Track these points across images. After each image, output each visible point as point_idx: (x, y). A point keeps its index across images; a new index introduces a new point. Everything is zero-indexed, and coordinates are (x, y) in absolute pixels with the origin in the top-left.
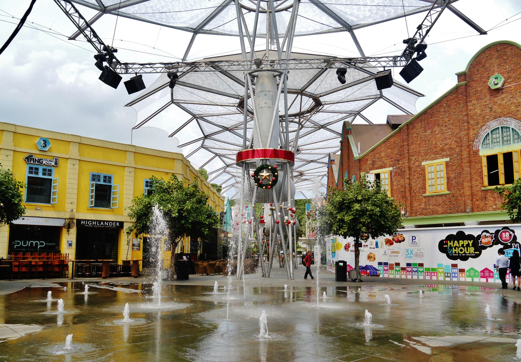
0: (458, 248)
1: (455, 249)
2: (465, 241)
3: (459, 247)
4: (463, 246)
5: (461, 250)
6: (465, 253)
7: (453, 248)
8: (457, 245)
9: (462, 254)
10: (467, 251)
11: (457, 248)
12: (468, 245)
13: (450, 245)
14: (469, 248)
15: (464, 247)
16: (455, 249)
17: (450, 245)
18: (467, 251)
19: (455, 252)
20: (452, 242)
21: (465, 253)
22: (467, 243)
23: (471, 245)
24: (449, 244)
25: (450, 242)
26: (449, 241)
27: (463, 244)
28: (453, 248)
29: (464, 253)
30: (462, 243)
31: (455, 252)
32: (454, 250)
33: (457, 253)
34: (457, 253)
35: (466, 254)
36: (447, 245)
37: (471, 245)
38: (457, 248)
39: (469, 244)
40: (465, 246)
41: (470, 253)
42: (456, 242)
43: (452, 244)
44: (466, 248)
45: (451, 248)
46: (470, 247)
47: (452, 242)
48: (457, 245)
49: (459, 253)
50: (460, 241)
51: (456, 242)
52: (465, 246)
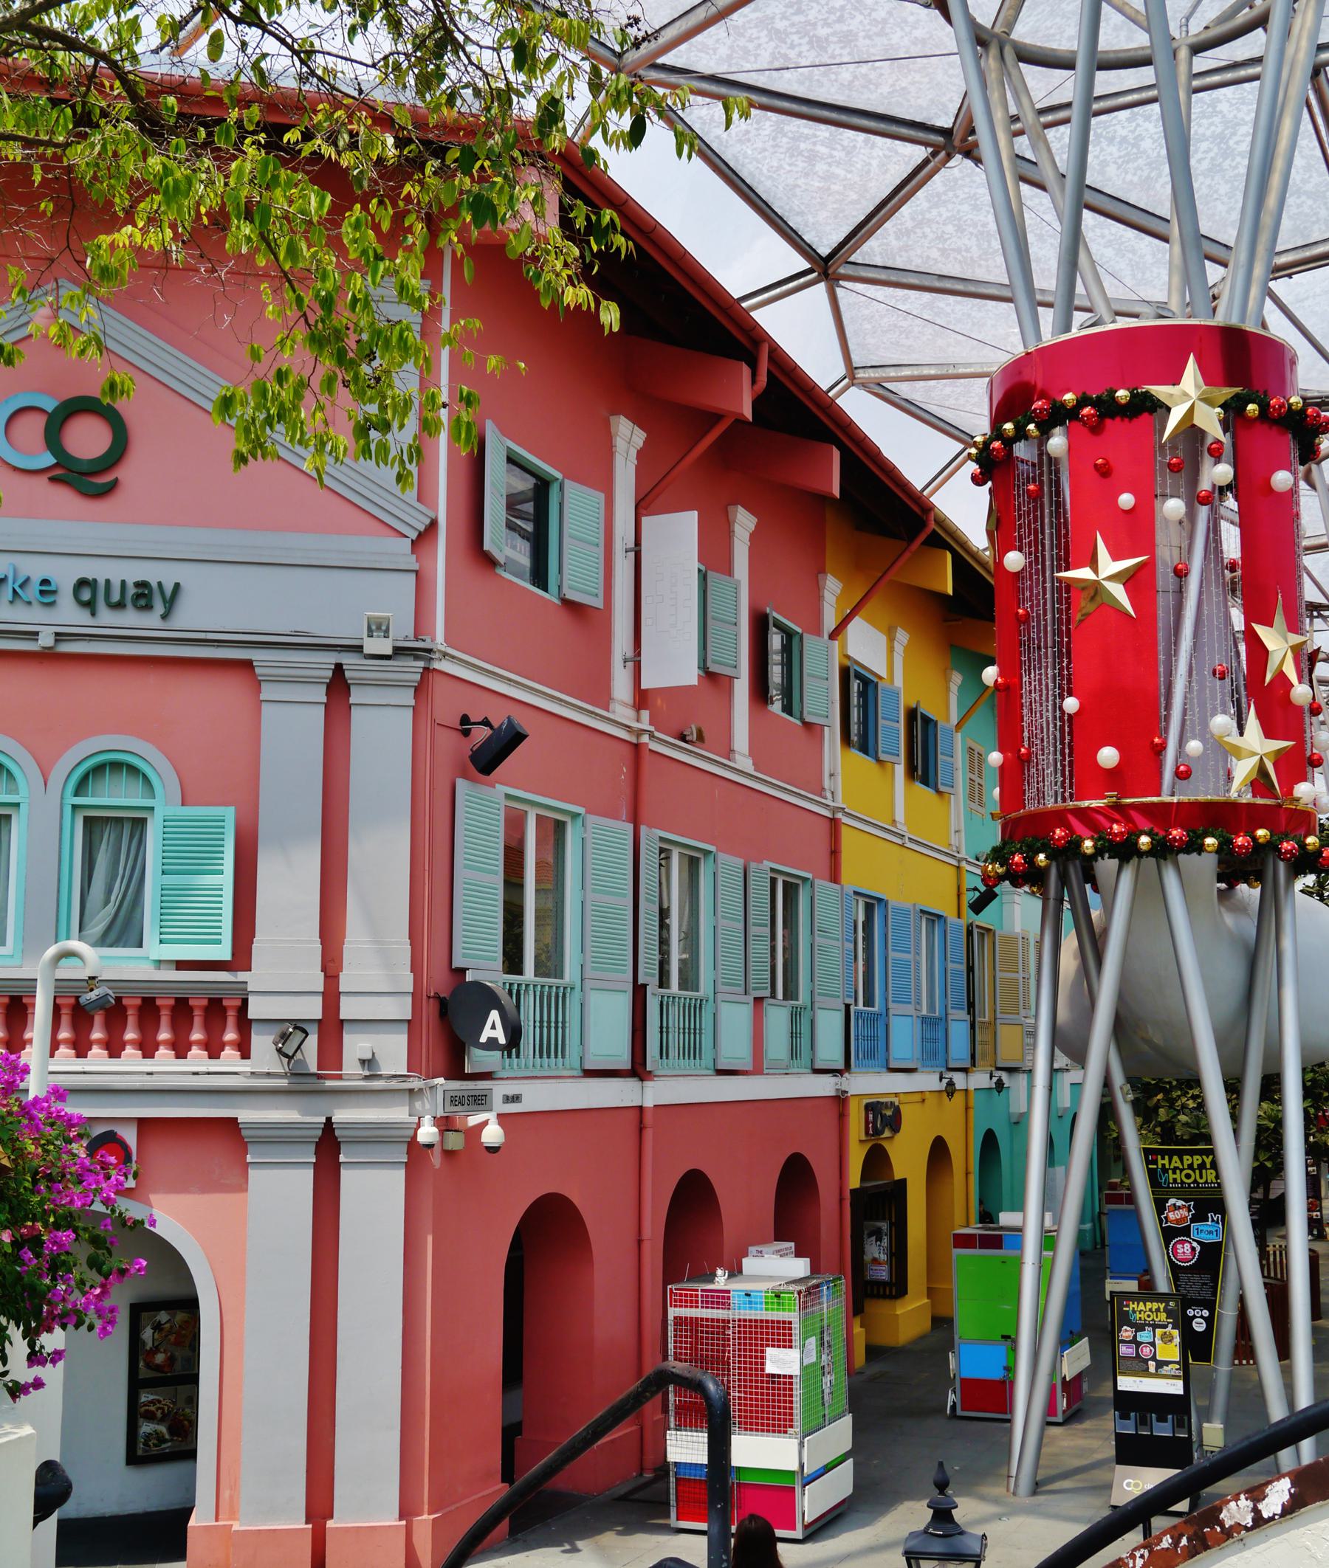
0: (1182, 1170)
1: (1174, 1173)
2: (1195, 1157)
3: (1184, 1169)
4: (1190, 1167)
5: (1188, 1176)
6: (1195, 1181)
7: (1170, 1172)
8: (1179, 1164)
9: (1189, 1184)
10: (1201, 1177)
11: (1178, 1171)
12: (1202, 1166)
13: (1163, 1165)
14: (1204, 1171)
15: (1194, 1171)
16: (1174, 1173)
17: (1163, 1165)
18: (1201, 1177)
19: (1175, 1180)
20: (1167, 1157)
21: (1195, 1181)
22: (1200, 1162)
23: (1208, 1166)
24: (1160, 1162)
25: (1163, 1159)
26: (1159, 1157)
27: (1192, 1163)
28: (1170, 1172)
29: (1193, 1183)
30: (1189, 1162)
31: (1175, 1180)
32: (1171, 1176)
33: (1179, 1181)
34: (1179, 1181)
35: (1198, 1183)
36: (1157, 1164)
37: (1208, 1166)
38: (1178, 1171)
39: (1204, 1162)
40: (1195, 1167)
41: (1206, 1182)
42: (1175, 1158)
43: (1166, 1161)
44: (1197, 1172)
45: (1165, 1170)
46: (1206, 1169)
47: (1167, 1157)
48: (1179, 1164)
49: (1182, 1182)
50: (1185, 1157)
51: (1175, 1158)
52: (1195, 1167)
